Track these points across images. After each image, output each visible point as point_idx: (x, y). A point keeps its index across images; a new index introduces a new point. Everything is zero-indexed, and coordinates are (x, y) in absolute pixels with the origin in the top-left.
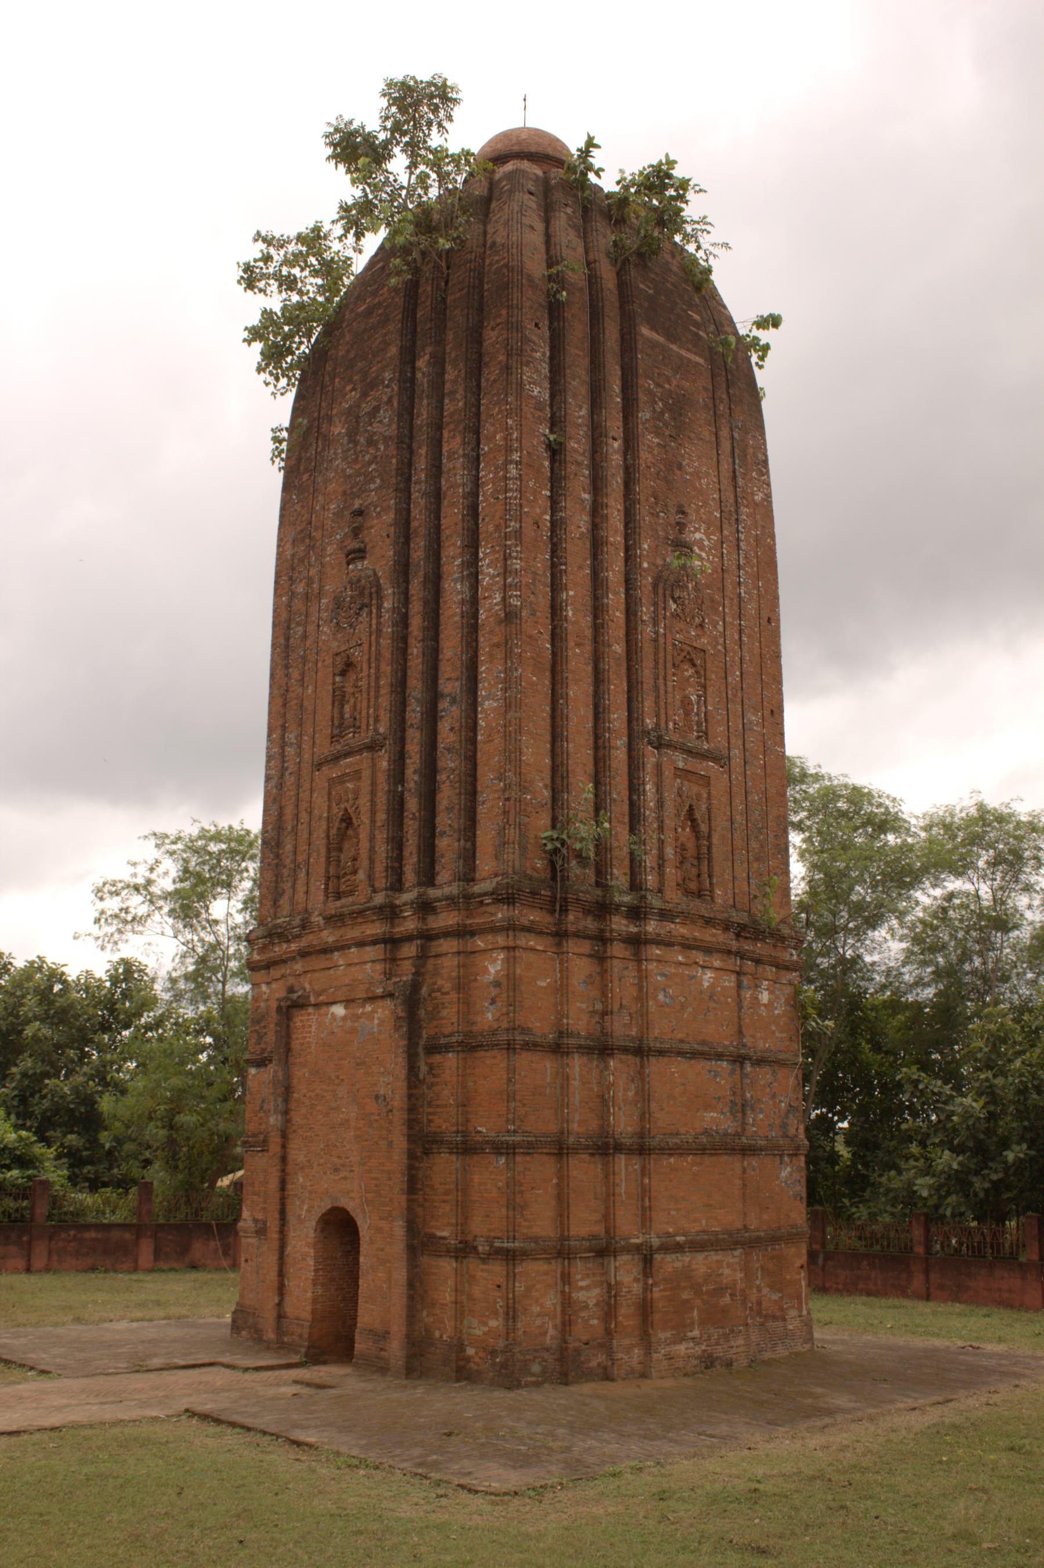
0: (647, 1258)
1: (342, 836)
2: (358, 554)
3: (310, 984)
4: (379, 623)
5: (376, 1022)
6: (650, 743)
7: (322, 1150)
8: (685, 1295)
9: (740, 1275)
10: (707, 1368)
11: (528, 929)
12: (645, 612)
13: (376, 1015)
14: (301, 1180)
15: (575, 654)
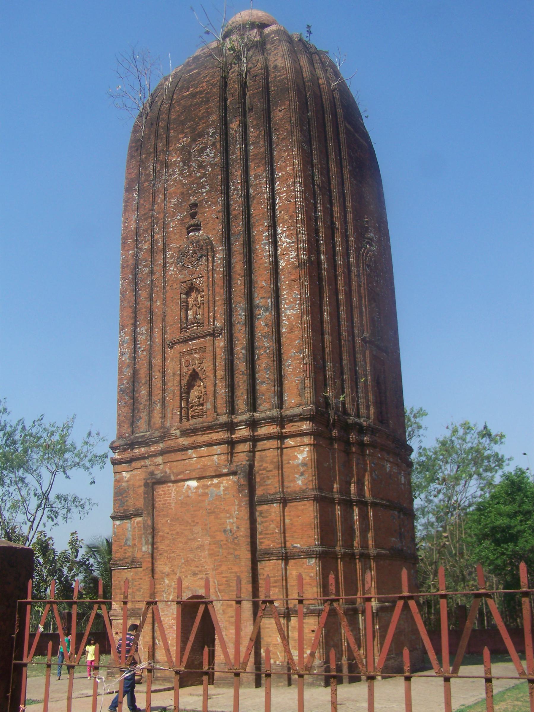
1: (190, 386)
2: (197, 227)
3: (170, 469)
4: (213, 266)
5: (222, 488)
7: (183, 563)
13: (222, 485)
14: (167, 582)
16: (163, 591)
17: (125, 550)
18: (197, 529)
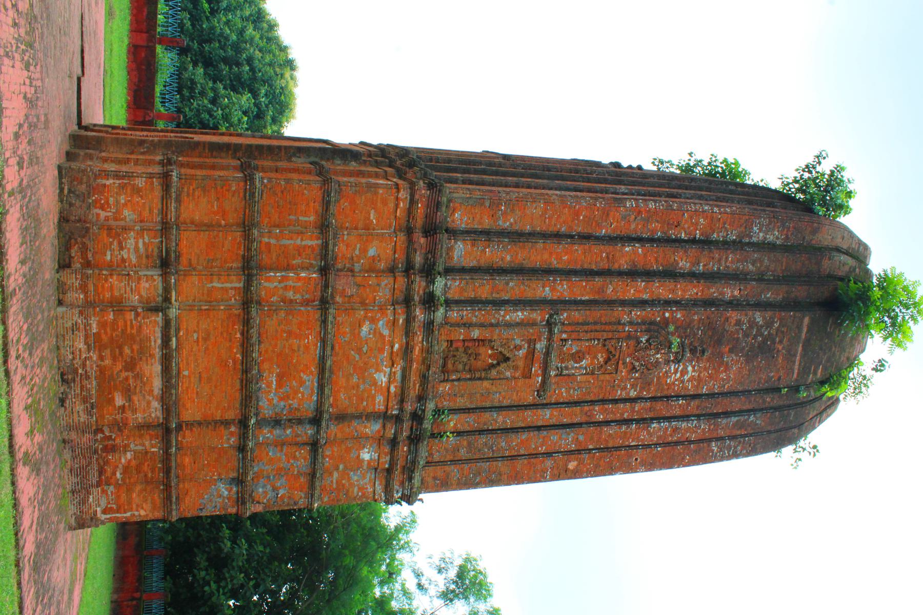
0: (160, 306)
6: (551, 316)
8: (127, 350)
9: (140, 417)
10: (62, 375)
11: (413, 202)
12: (637, 313)
15: (602, 252)
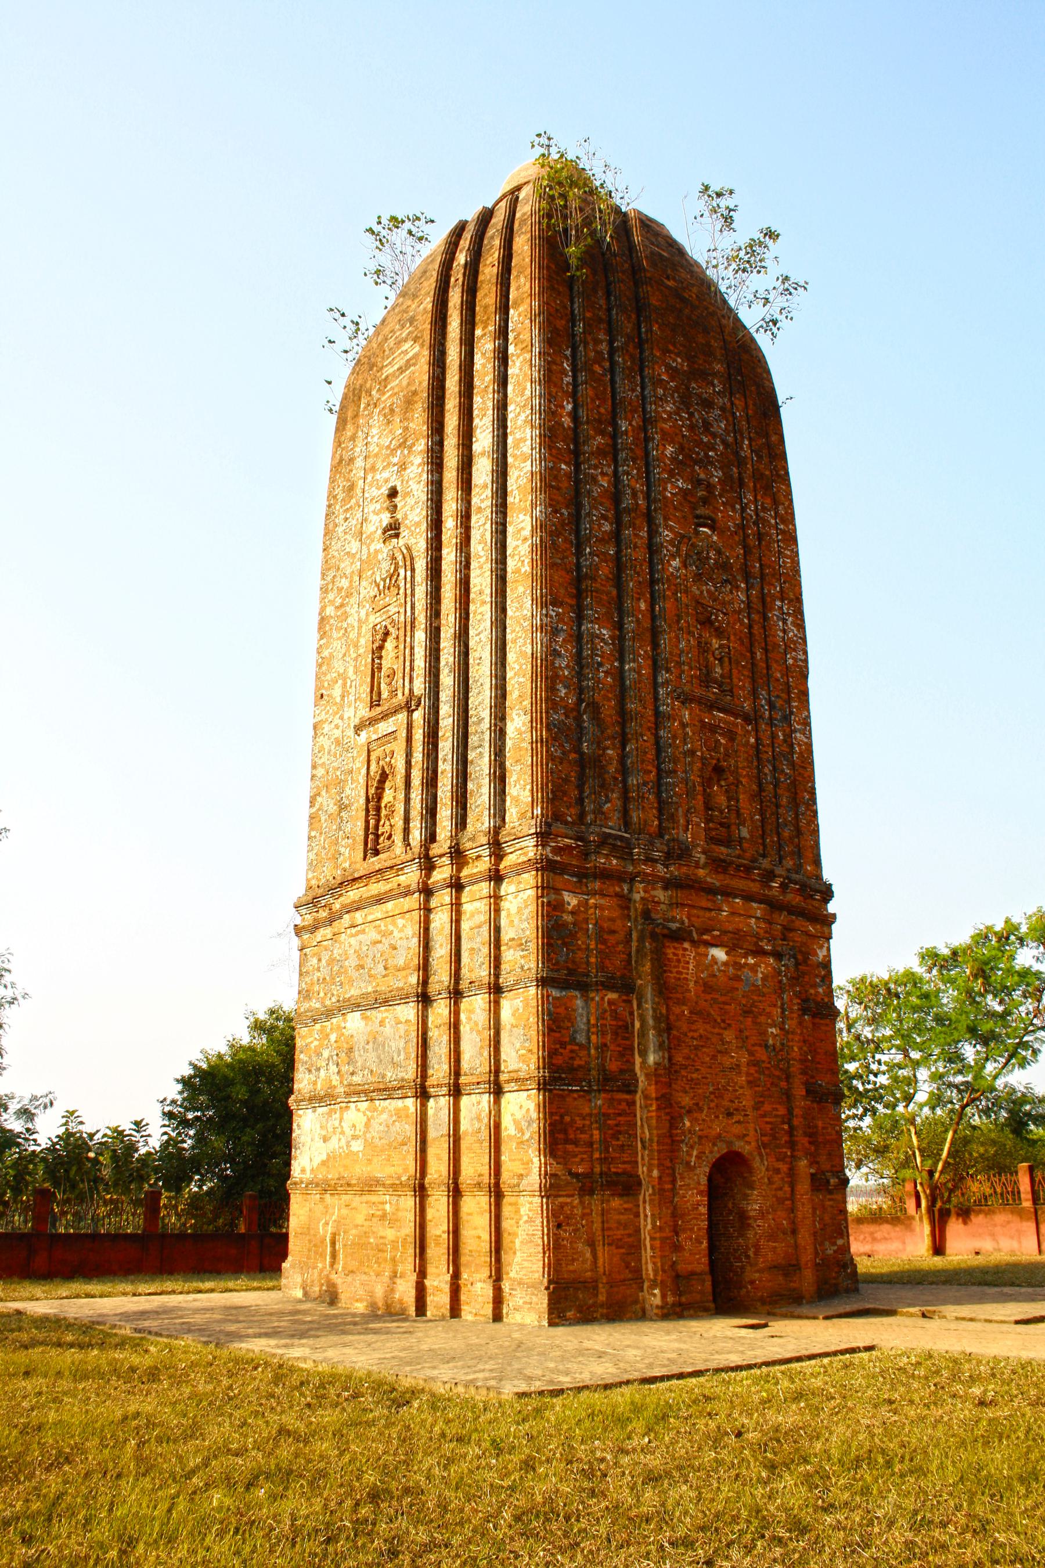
7: (711, 1093)
14: (688, 1124)
16: (682, 1141)
17: (572, 1051)
18: (729, 1036)
